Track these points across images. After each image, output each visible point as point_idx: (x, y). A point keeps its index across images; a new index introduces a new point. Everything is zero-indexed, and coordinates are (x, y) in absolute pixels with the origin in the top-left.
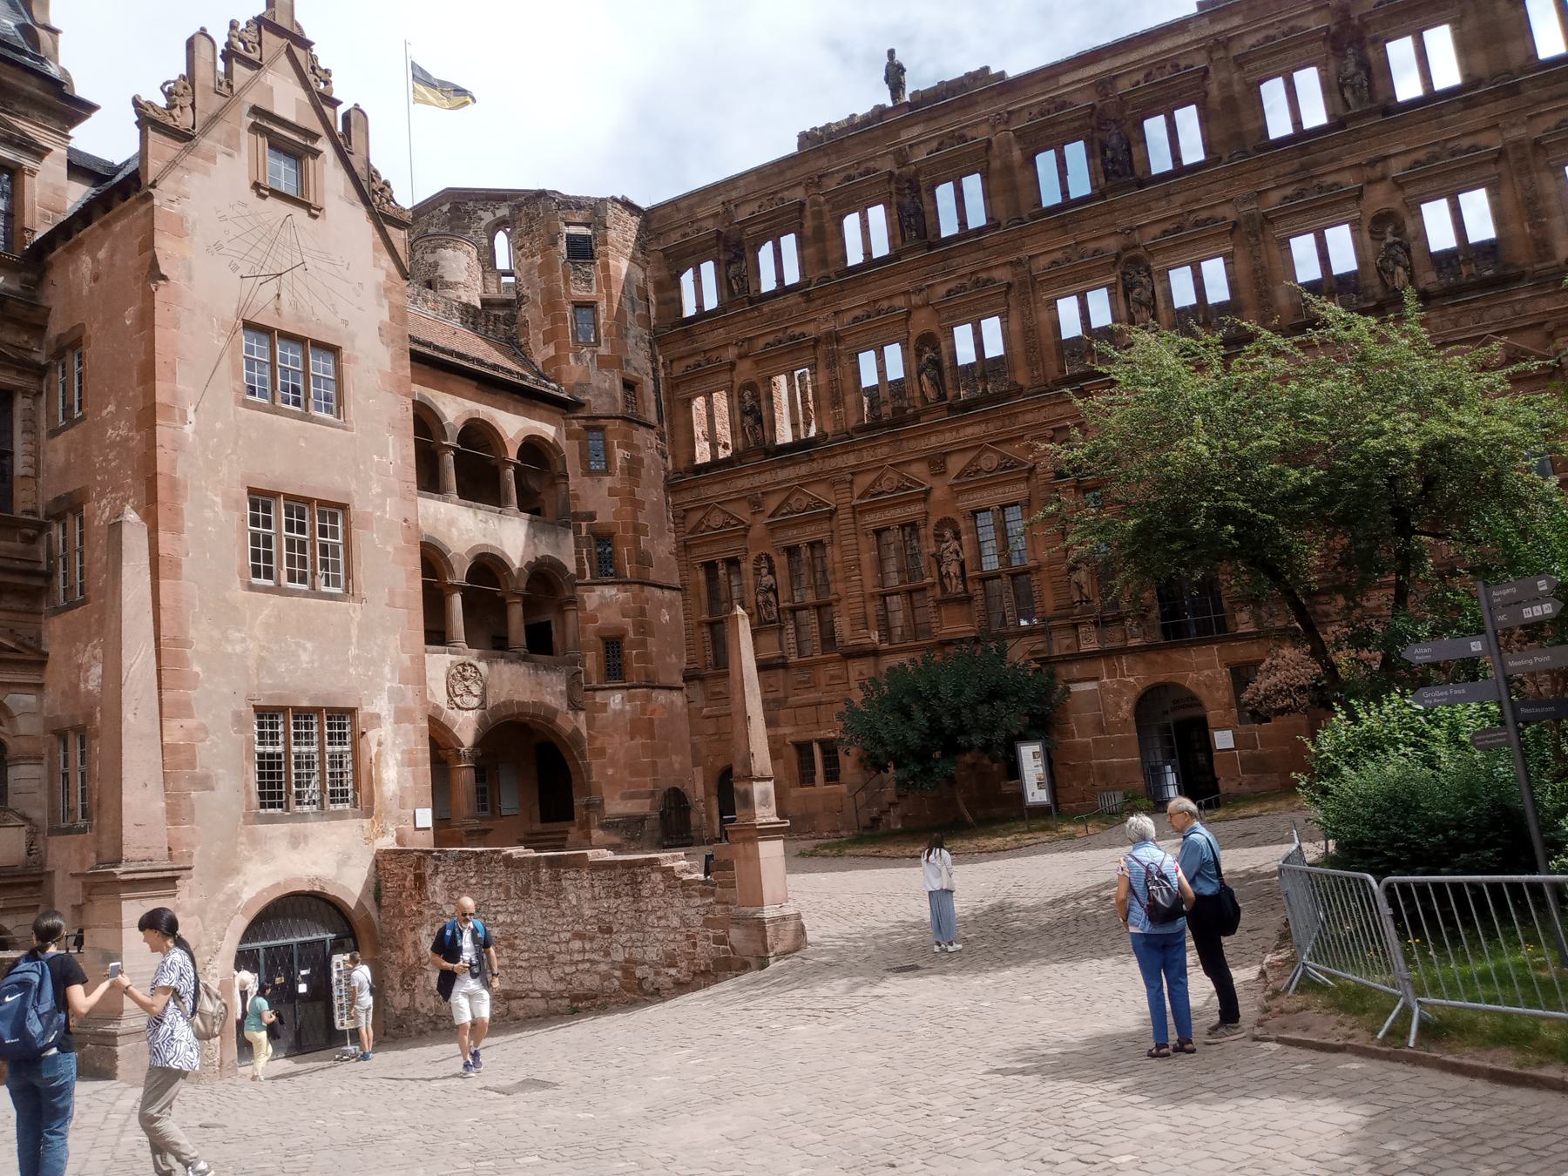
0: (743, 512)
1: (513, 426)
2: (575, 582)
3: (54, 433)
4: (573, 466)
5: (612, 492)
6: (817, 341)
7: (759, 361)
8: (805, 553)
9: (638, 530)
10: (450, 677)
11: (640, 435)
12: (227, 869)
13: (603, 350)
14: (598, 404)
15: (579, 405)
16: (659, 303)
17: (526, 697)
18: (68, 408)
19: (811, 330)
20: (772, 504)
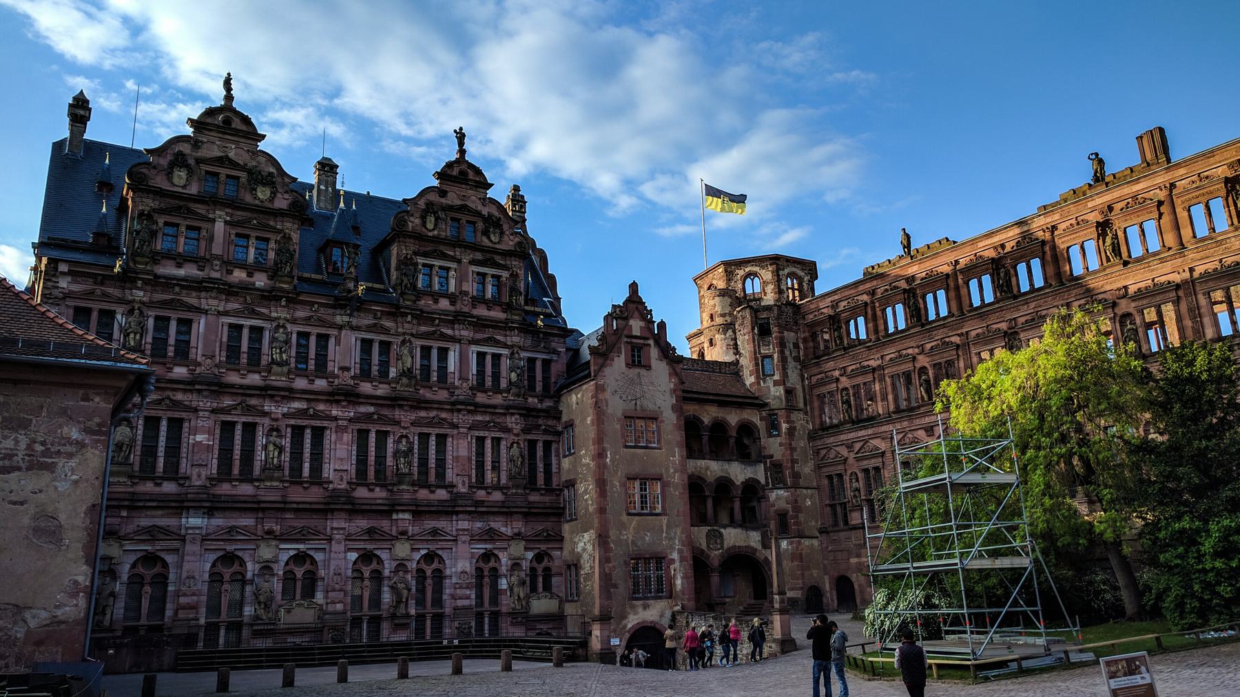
0: (844, 452)
1: (733, 418)
2: (764, 488)
3: (565, 456)
4: (763, 433)
5: (781, 445)
6: (874, 370)
7: (850, 377)
8: (872, 473)
9: (794, 462)
10: (707, 535)
11: (795, 416)
12: (624, 616)
13: (777, 377)
14: (774, 404)
15: (766, 404)
16: (806, 348)
17: (742, 544)
18: (569, 449)
19: (873, 363)
20: (857, 446)
